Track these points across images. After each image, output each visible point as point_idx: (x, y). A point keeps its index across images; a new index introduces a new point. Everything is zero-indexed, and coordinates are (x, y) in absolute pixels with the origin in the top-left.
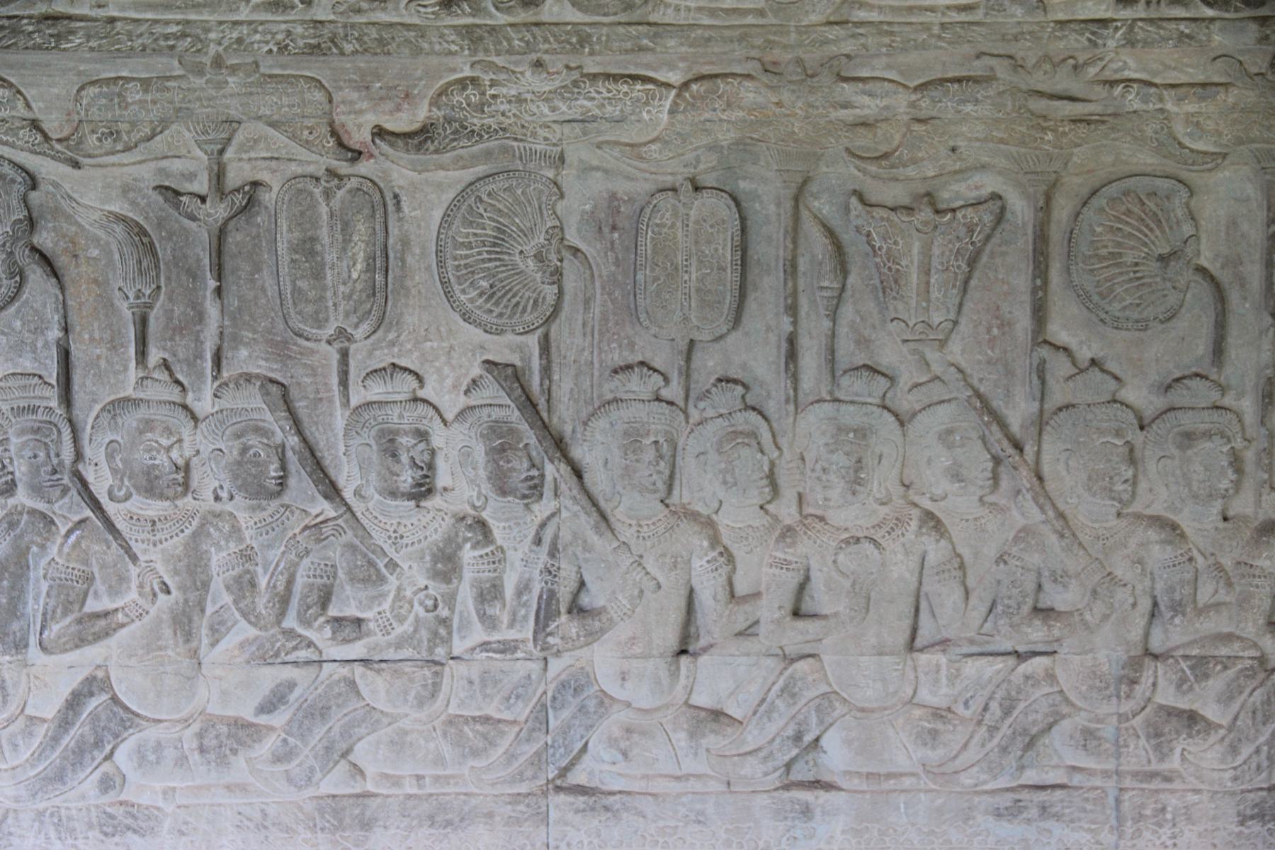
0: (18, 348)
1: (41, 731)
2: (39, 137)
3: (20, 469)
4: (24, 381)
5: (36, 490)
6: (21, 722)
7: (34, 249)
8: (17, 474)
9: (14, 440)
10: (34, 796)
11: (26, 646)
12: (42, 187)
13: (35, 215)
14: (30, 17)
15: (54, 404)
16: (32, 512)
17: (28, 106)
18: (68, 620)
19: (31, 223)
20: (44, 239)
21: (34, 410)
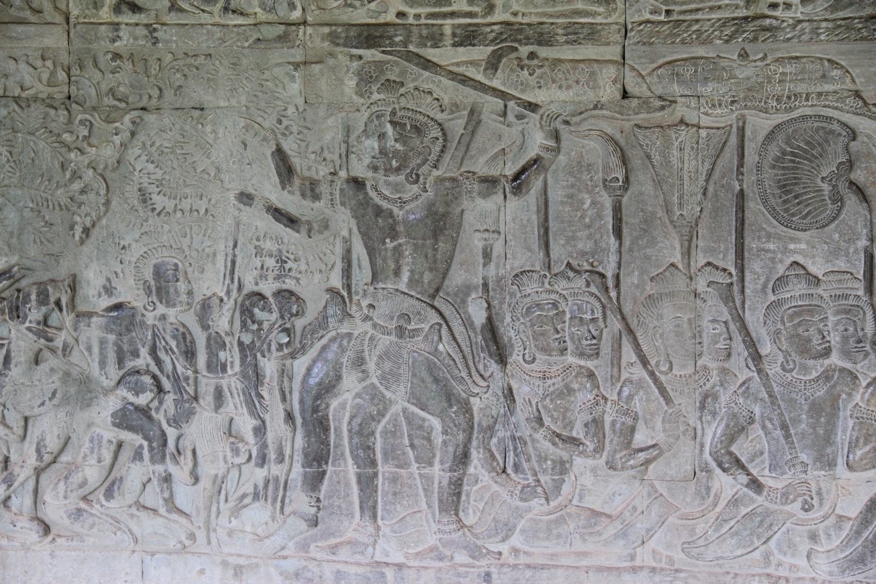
0: (835, 253)
1: (848, 526)
2: (860, 103)
3: (835, 339)
4: (840, 277)
5: (846, 354)
6: (832, 520)
7: (852, 183)
8: (833, 343)
9: (831, 318)
10: (843, 572)
11: (835, 465)
12: (859, 139)
13: (853, 158)
14: (860, 18)
15: (861, 293)
16: (842, 370)
17: (853, 81)
18: (867, 448)
19: (850, 164)
20: (859, 175)
21: (847, 297)
